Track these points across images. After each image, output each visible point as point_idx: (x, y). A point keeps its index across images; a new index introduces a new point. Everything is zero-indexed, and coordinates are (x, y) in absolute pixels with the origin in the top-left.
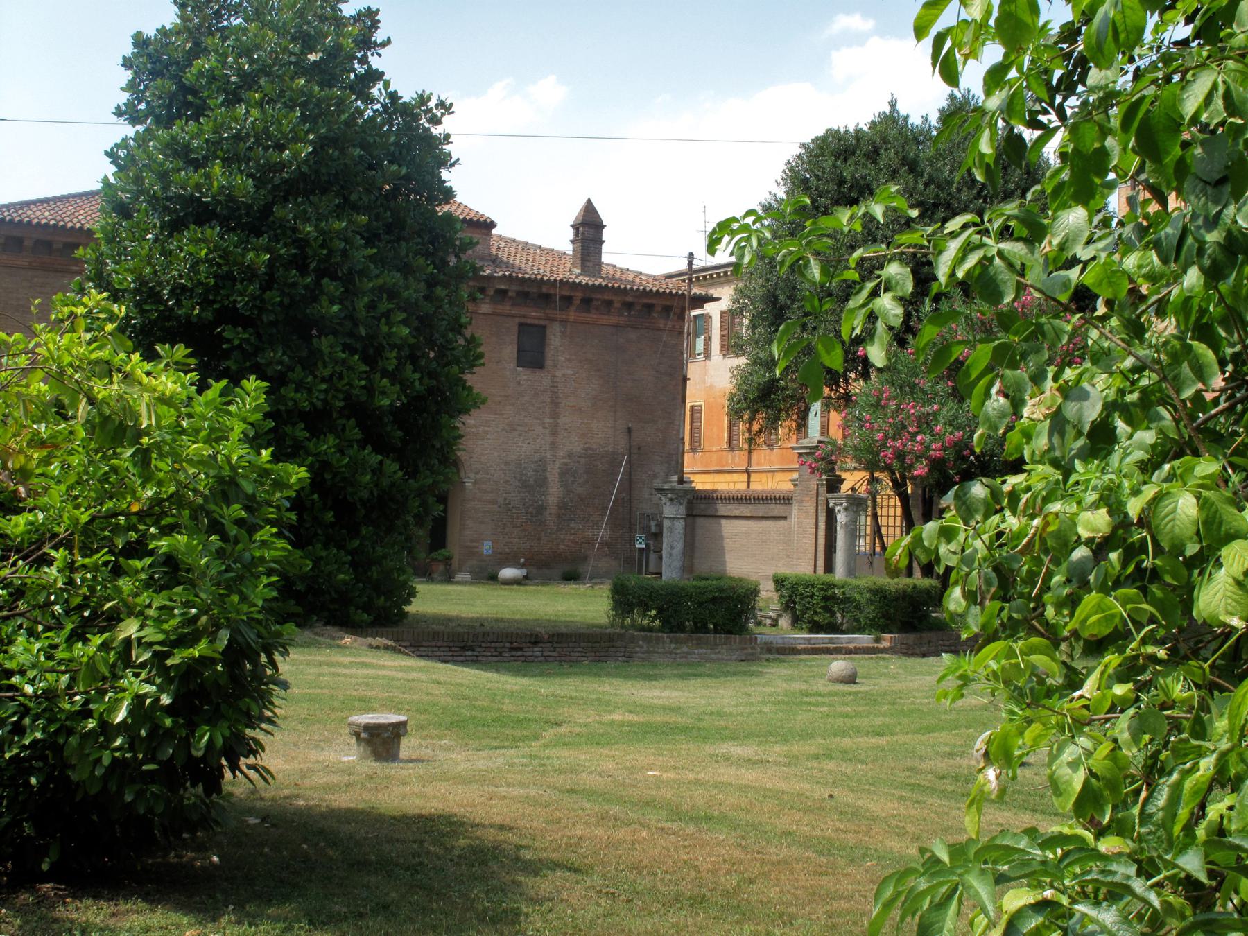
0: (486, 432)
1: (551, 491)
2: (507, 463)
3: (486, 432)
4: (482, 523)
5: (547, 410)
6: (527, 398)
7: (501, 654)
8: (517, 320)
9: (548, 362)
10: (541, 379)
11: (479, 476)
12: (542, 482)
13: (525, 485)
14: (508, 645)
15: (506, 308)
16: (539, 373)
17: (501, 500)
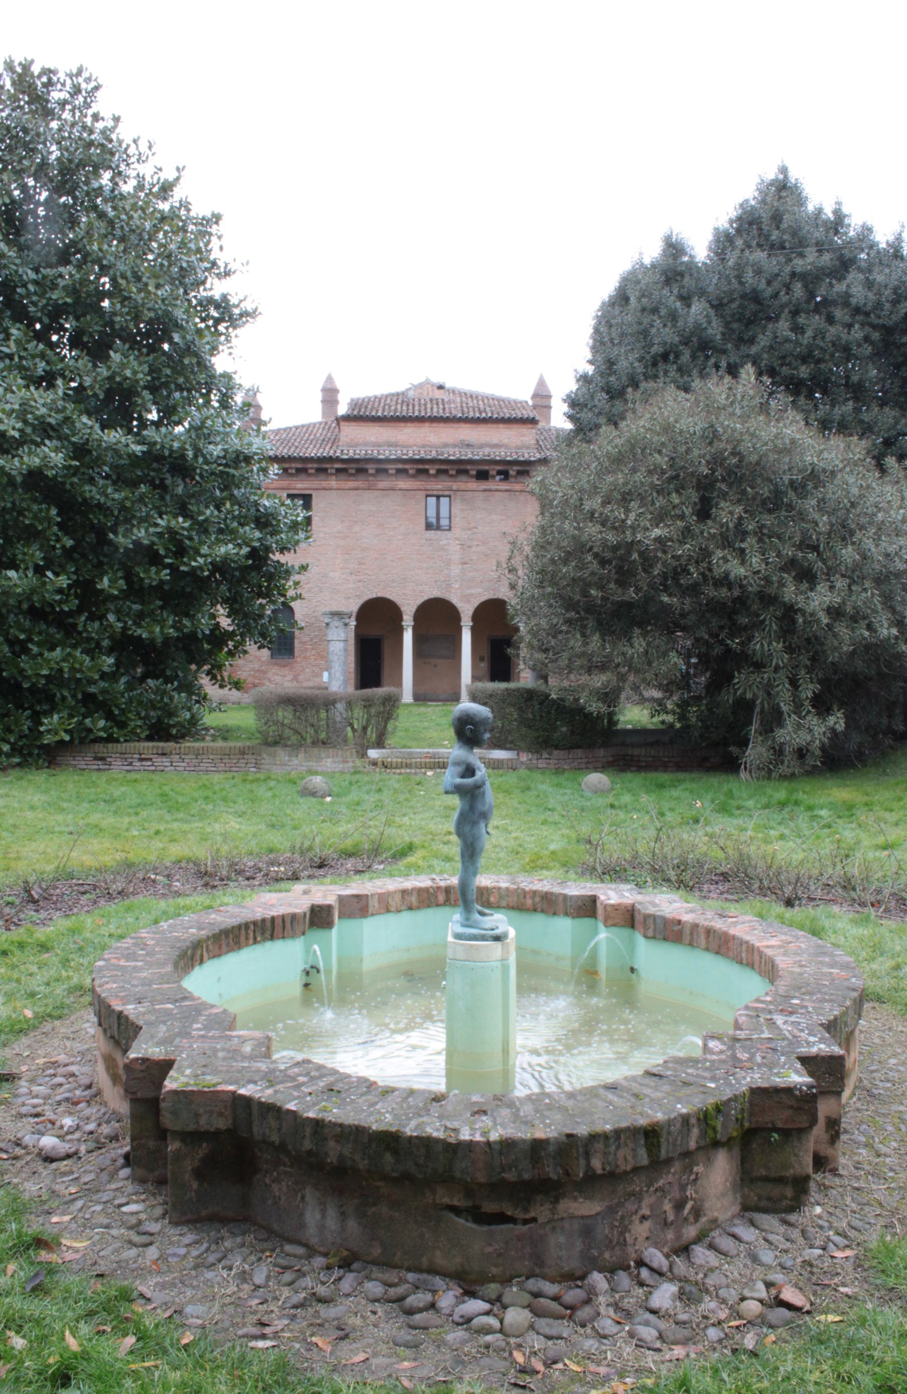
7: (131, 764)
14: (137, 756)
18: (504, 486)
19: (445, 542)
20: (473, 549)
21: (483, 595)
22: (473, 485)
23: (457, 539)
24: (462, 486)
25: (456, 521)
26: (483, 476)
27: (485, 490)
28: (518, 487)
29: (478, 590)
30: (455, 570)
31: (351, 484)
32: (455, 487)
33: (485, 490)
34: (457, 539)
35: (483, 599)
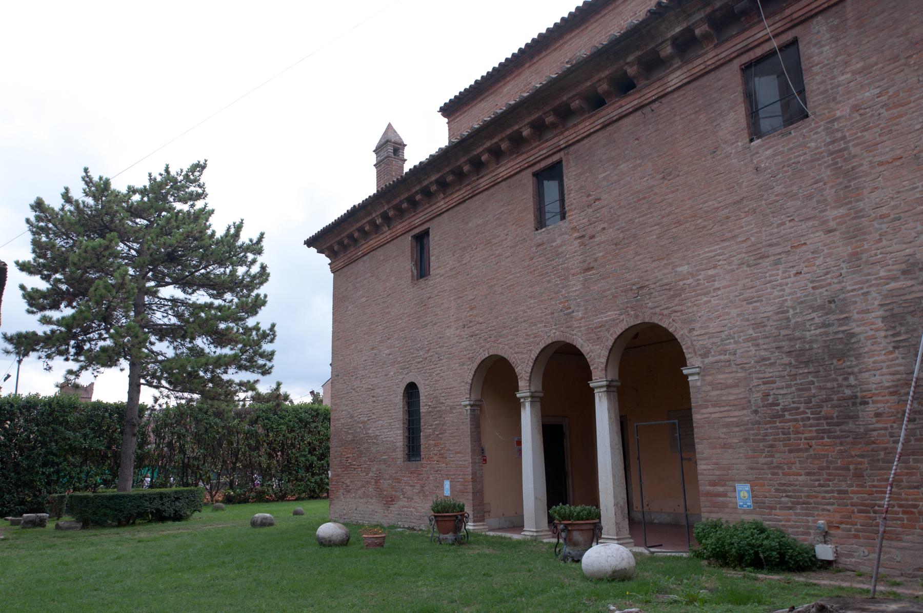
0: (711, 279)
1: (869, 361)
2: (758, 325)
3: (711, 279)
4: (726, 446)
5: (829, 193)
6: (779, 189)
8: (736, 64)
9: (814, 101)
10: (810, 137)
11: (711, 359)
12: (843, 349)
13: (802, 357)
15: (709, 56)
16: (798, 132)
17: (756, 397)
18: (629, 102)
19: (559, 241)
20: (597, 239)
21: (618, 321)
22: (585, 126)
23: (574, 229)
24: (570, 135)
25: (571, 199)
26: (597, 102)
27: (604, 127)
28: (651, 93)
29: (612, 314)
30: (576, 283)
31: (457, 197)
32: (562, 143)
33: (604, 127)
34: (574, 229)
35: (619, 331)
